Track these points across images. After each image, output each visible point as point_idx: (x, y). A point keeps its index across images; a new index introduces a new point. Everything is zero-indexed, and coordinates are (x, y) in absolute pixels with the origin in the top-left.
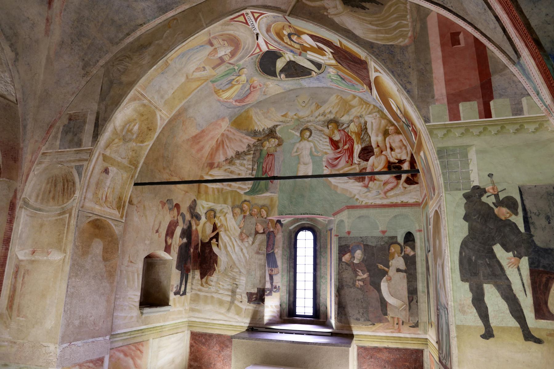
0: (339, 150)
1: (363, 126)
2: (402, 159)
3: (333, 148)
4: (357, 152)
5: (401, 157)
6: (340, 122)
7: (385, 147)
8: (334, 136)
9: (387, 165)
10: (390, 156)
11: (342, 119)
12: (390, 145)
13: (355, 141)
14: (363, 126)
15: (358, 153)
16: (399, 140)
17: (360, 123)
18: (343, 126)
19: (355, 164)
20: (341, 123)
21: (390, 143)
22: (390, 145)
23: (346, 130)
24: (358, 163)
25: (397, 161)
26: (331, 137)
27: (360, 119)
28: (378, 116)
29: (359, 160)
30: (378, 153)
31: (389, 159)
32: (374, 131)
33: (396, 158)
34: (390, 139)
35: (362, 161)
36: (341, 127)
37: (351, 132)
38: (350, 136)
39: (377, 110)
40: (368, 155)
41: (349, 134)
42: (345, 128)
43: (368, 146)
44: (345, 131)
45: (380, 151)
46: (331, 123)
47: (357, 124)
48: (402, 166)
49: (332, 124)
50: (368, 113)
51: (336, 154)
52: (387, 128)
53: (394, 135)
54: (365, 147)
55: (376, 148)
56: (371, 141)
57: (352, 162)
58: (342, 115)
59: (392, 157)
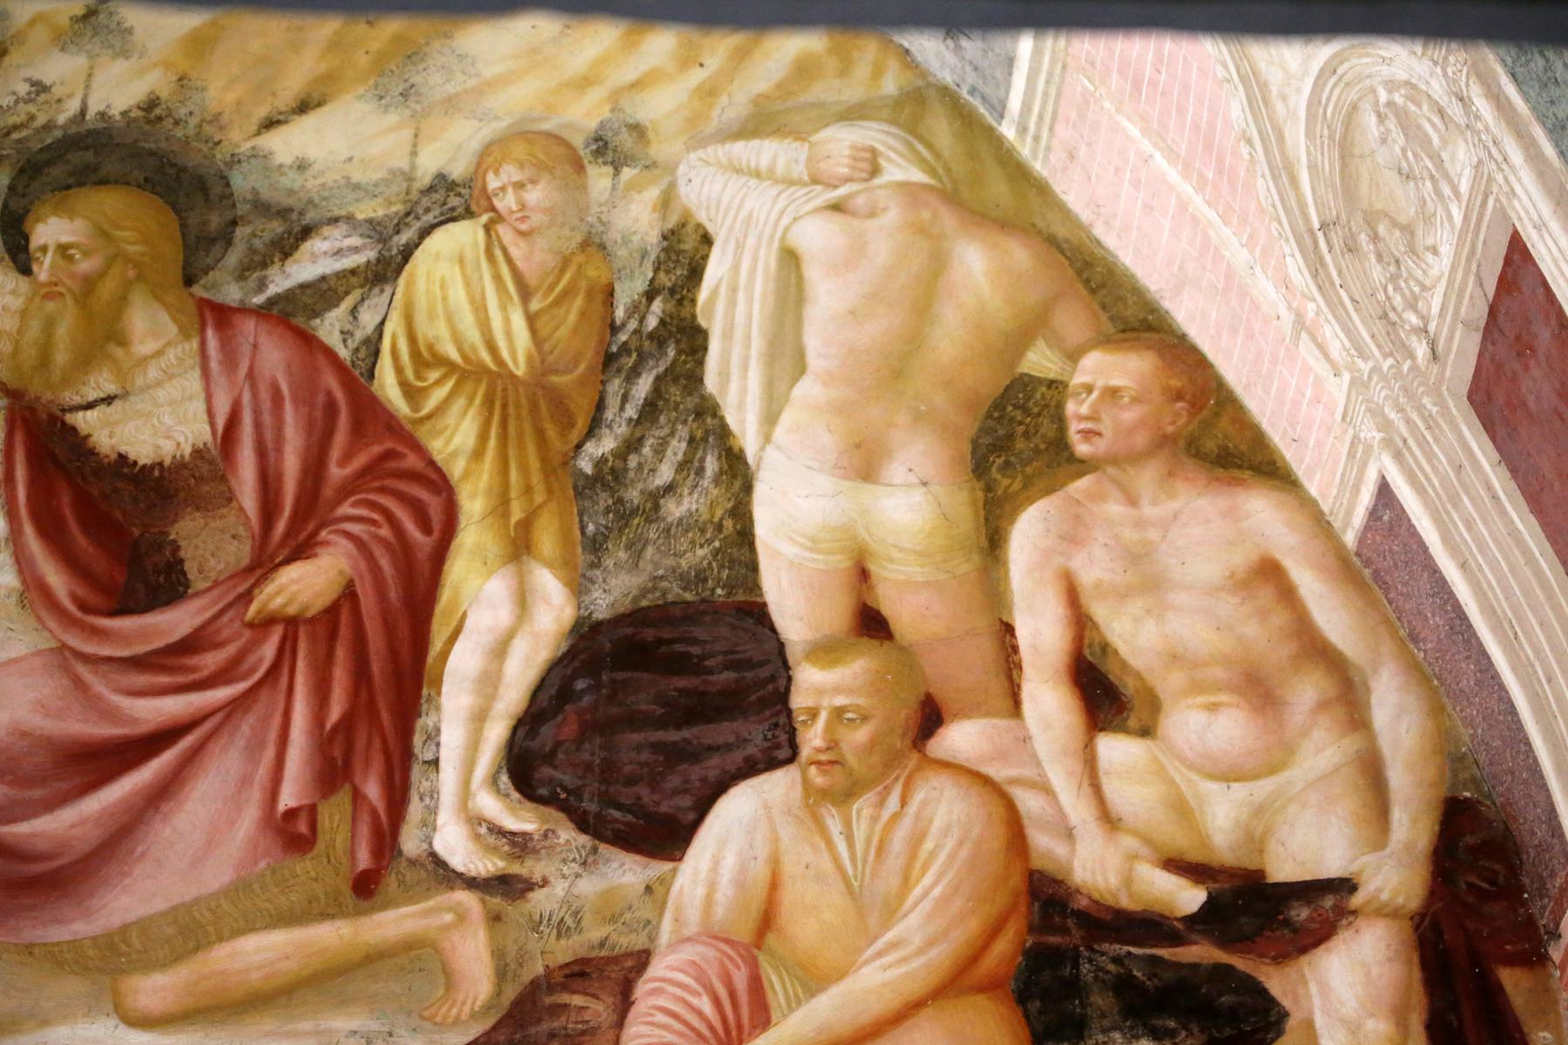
0: (176, 621)
1: (628, 292)
2: (1284, 868)
3: (57, 579)
4: (489, 683)
5: (1256, 840)
6: (242, 182)
7: (984, 650)
8: (101, 383)
9: (1004, 948)
10: (1077, 807)
11: (284, 145)
12: (1080, 622)
13: (473, 504)
14: (628, 292)
15: (513, 695)
16: (1241, 559)
17: (594, 245)
18: (286, 247)
19: (441, 873)
20: (263, 208)
21: (1073, 596)
22: (1080, 622)
23: (330, 328)
24: (483, 865)
25: (1189, 897)
26: (36, 388)
27: (599, 179)
28: (899, 170)
29: (523, 820)
30: (862, 734)
31: (1044, 843)
32: (807, 390)
33: (1180, 841)
34: (1073, 535)
35: (568, 835)
36: (257, 264)
37: (425, 358)
38: (392, 426)
39: (890, 84)
40: (677, 755)
41: (387, 385)
42: (323, 293)
43: (691, 614)
44: (308, 342)
45: (906, 712)
46: (88, 177)
47: (533, 257)
48: (1276, 982)
49: (109, 202)
50: (734, 104)
51: (97, 684)
52: (1040, 361)
53: (1146, 478)
54: (635, 617)
55: (824, 652)
56: (746, 536)
57: (386, 841)
58: (292, 84)
59: (1109, 819)
